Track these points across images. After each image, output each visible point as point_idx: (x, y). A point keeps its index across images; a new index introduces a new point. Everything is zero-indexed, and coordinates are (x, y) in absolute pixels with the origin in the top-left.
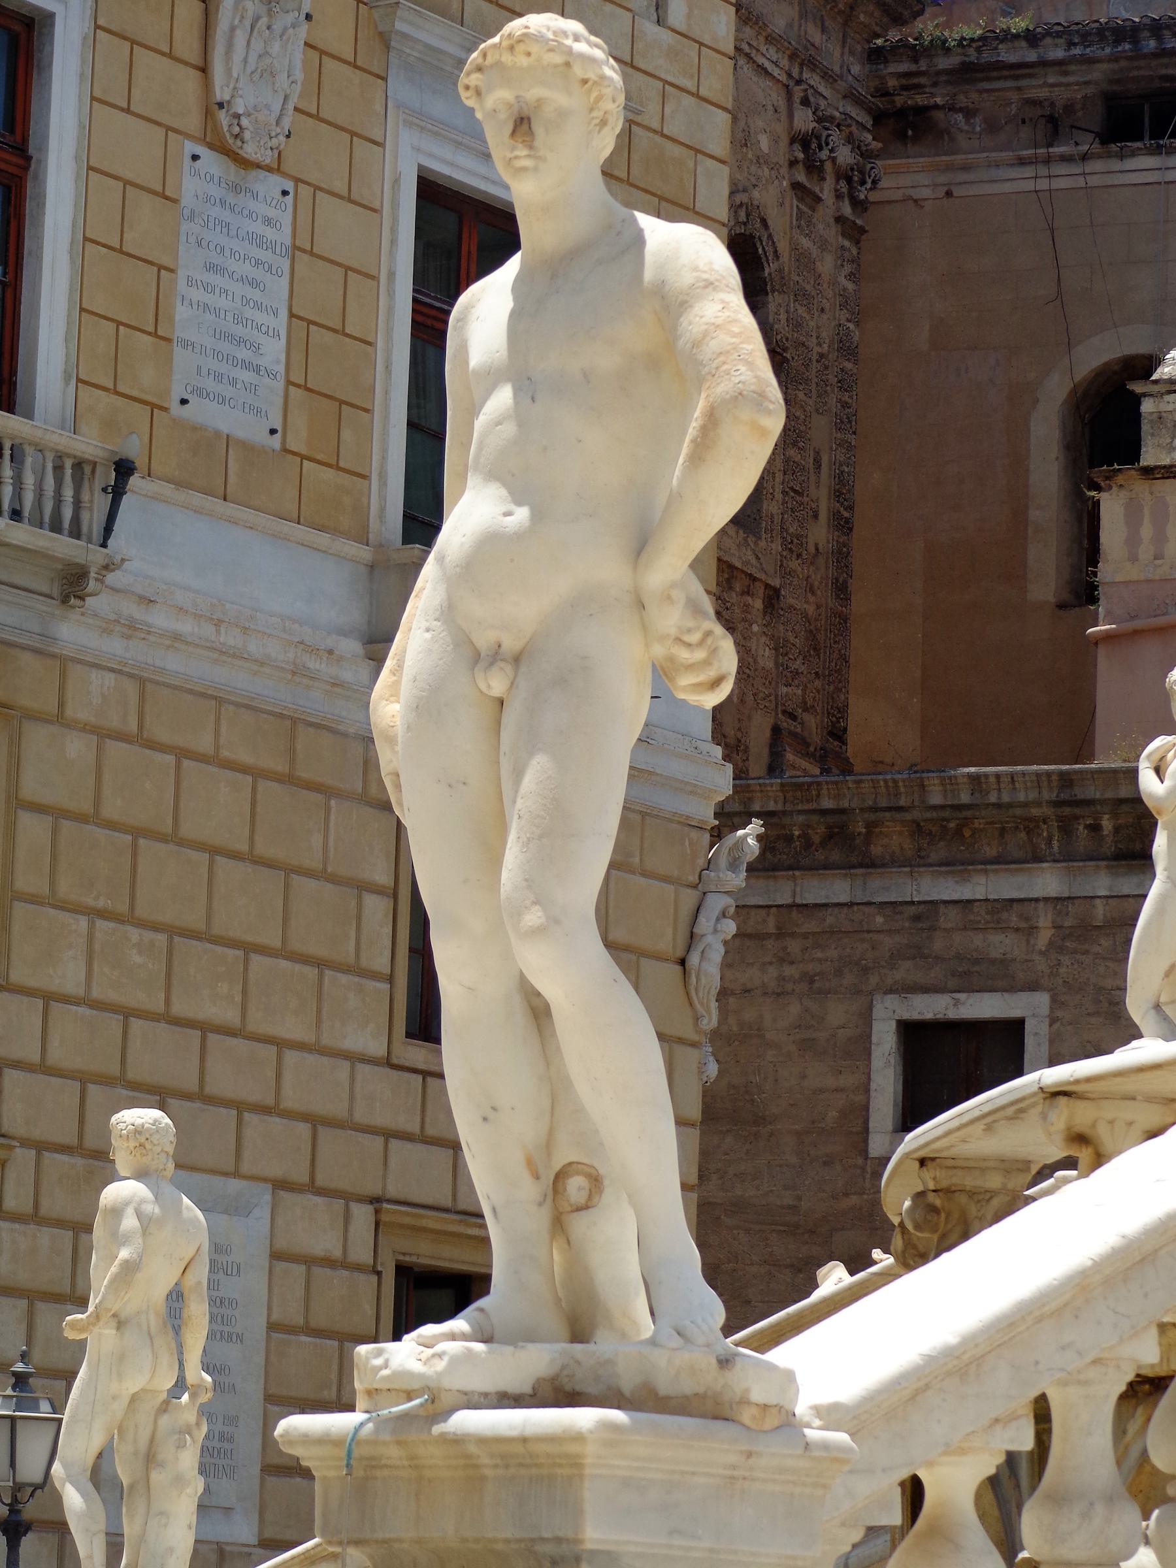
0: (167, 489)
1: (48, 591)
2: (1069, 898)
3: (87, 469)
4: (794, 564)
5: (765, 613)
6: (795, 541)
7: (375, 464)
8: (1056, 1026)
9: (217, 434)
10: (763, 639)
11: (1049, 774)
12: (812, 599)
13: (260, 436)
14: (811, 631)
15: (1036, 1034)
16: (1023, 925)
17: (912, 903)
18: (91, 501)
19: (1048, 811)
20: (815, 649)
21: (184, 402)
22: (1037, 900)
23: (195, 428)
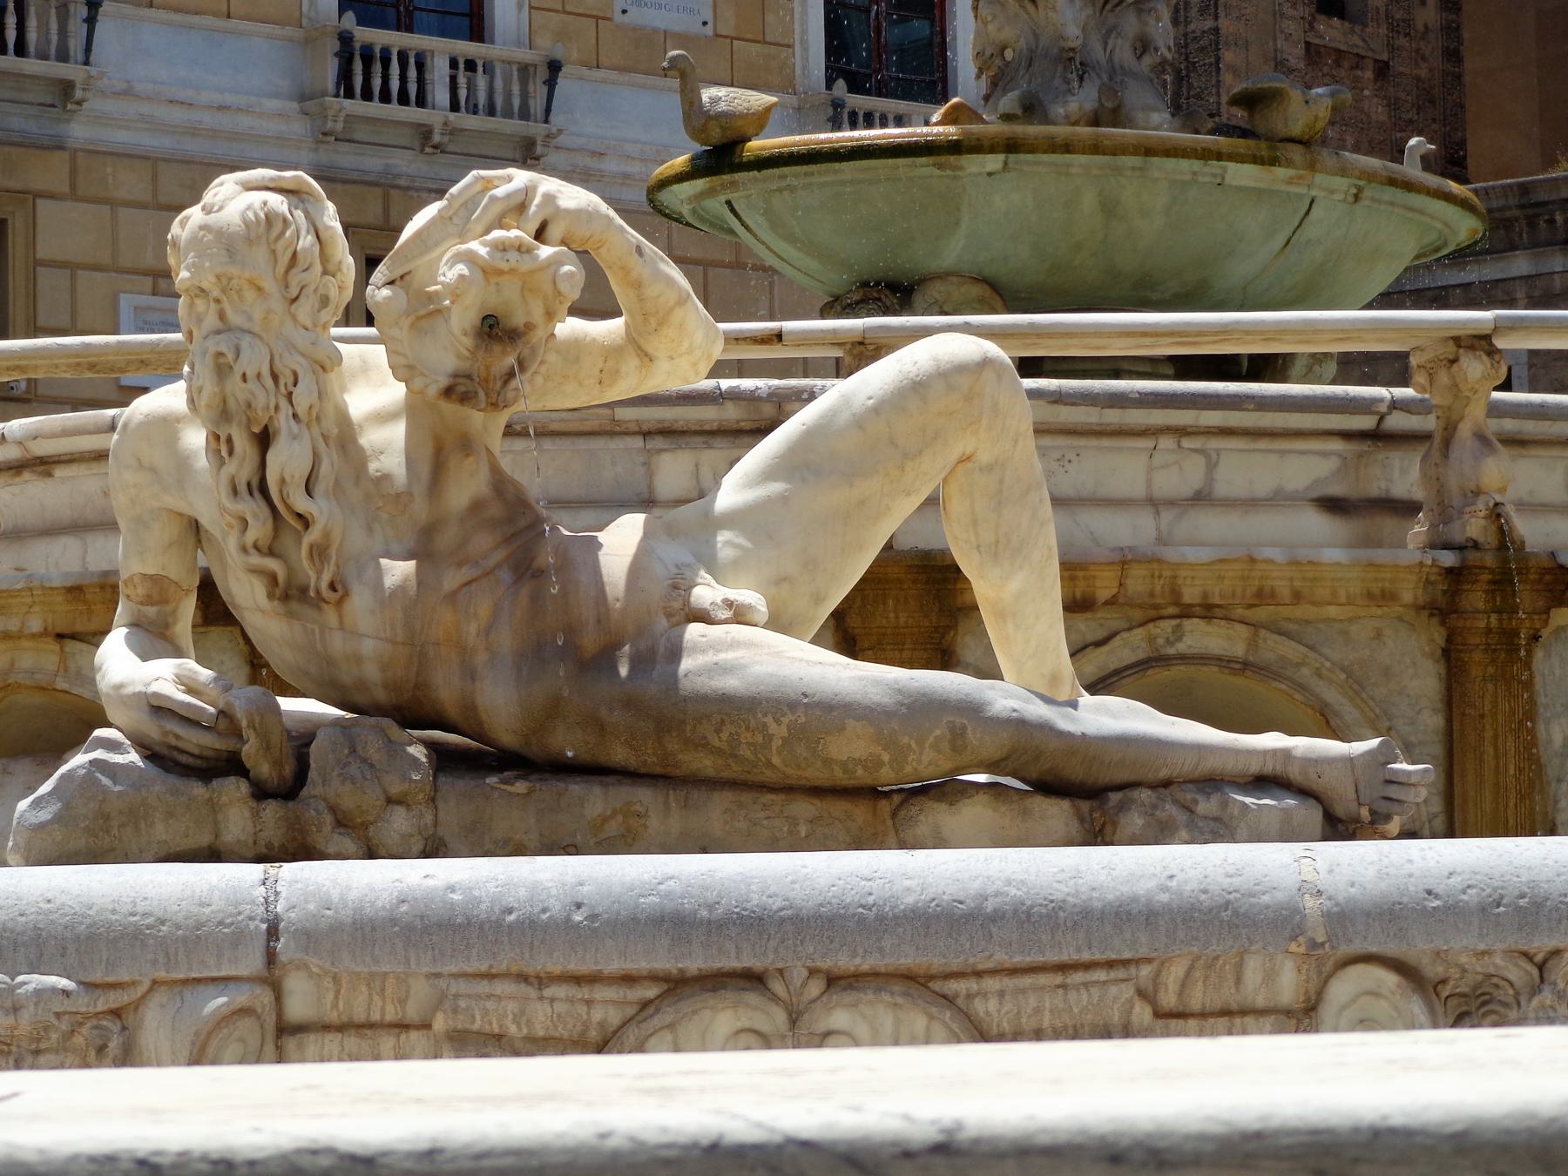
0: (613, 75)
1: (511, 157)
2: (1536, 275)
3: (531, 70)
4: (1402, 41)
5: (1376, 80)
6: (1402, 24)
7: (797, 36)
8: (1533, 370)
9: (655, 31)
10: (1375, 100)
11: (1510, 186)
12: (1424, 65)
13: (696, 28)
14: (1424, 89)
15: (1519, 377)
16: (1505, 298)
17: (1429, 289)
18: (535, 92)
19: (1516, 213)
20: (1430, 102)
21: (624, 12)
22: (1514, 279)
23: (634, 29)
